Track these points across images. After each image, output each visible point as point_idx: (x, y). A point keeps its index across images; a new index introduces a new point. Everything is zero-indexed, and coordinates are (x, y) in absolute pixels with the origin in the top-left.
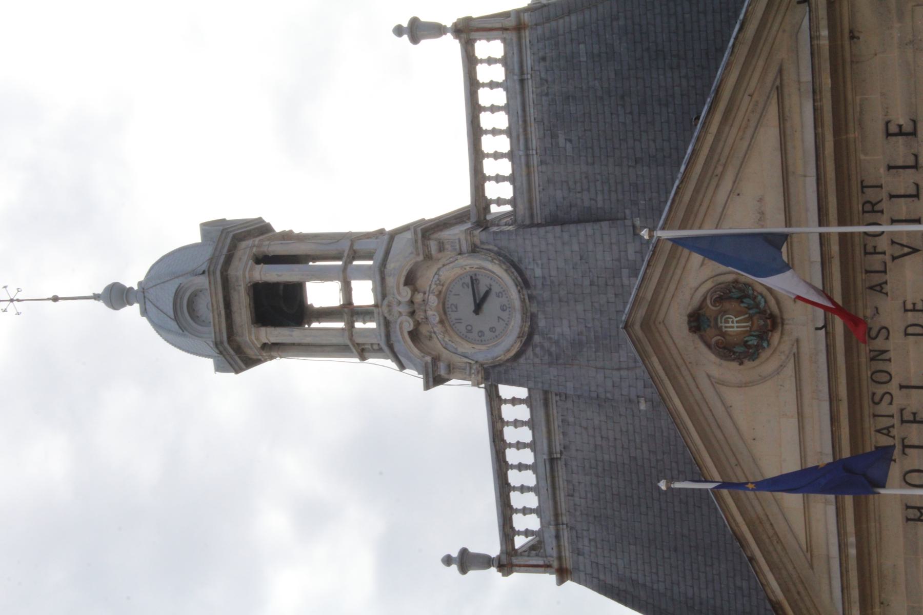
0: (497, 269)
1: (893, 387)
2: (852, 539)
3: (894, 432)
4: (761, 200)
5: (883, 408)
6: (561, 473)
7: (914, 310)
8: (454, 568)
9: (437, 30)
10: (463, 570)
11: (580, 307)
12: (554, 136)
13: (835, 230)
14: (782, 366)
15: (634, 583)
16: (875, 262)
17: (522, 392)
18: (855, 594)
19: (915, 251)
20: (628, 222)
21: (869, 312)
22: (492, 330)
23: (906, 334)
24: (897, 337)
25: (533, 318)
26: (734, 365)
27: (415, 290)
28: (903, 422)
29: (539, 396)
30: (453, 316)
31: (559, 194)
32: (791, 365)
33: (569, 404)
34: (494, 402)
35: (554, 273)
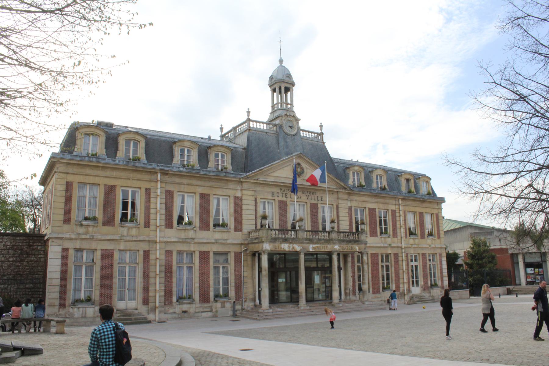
5: (287, 191)
6: (265, 134)
9: (321, 130)
13: (327, 189)
16: (306, 193)
18: (265, 182)
30: (288, 122)
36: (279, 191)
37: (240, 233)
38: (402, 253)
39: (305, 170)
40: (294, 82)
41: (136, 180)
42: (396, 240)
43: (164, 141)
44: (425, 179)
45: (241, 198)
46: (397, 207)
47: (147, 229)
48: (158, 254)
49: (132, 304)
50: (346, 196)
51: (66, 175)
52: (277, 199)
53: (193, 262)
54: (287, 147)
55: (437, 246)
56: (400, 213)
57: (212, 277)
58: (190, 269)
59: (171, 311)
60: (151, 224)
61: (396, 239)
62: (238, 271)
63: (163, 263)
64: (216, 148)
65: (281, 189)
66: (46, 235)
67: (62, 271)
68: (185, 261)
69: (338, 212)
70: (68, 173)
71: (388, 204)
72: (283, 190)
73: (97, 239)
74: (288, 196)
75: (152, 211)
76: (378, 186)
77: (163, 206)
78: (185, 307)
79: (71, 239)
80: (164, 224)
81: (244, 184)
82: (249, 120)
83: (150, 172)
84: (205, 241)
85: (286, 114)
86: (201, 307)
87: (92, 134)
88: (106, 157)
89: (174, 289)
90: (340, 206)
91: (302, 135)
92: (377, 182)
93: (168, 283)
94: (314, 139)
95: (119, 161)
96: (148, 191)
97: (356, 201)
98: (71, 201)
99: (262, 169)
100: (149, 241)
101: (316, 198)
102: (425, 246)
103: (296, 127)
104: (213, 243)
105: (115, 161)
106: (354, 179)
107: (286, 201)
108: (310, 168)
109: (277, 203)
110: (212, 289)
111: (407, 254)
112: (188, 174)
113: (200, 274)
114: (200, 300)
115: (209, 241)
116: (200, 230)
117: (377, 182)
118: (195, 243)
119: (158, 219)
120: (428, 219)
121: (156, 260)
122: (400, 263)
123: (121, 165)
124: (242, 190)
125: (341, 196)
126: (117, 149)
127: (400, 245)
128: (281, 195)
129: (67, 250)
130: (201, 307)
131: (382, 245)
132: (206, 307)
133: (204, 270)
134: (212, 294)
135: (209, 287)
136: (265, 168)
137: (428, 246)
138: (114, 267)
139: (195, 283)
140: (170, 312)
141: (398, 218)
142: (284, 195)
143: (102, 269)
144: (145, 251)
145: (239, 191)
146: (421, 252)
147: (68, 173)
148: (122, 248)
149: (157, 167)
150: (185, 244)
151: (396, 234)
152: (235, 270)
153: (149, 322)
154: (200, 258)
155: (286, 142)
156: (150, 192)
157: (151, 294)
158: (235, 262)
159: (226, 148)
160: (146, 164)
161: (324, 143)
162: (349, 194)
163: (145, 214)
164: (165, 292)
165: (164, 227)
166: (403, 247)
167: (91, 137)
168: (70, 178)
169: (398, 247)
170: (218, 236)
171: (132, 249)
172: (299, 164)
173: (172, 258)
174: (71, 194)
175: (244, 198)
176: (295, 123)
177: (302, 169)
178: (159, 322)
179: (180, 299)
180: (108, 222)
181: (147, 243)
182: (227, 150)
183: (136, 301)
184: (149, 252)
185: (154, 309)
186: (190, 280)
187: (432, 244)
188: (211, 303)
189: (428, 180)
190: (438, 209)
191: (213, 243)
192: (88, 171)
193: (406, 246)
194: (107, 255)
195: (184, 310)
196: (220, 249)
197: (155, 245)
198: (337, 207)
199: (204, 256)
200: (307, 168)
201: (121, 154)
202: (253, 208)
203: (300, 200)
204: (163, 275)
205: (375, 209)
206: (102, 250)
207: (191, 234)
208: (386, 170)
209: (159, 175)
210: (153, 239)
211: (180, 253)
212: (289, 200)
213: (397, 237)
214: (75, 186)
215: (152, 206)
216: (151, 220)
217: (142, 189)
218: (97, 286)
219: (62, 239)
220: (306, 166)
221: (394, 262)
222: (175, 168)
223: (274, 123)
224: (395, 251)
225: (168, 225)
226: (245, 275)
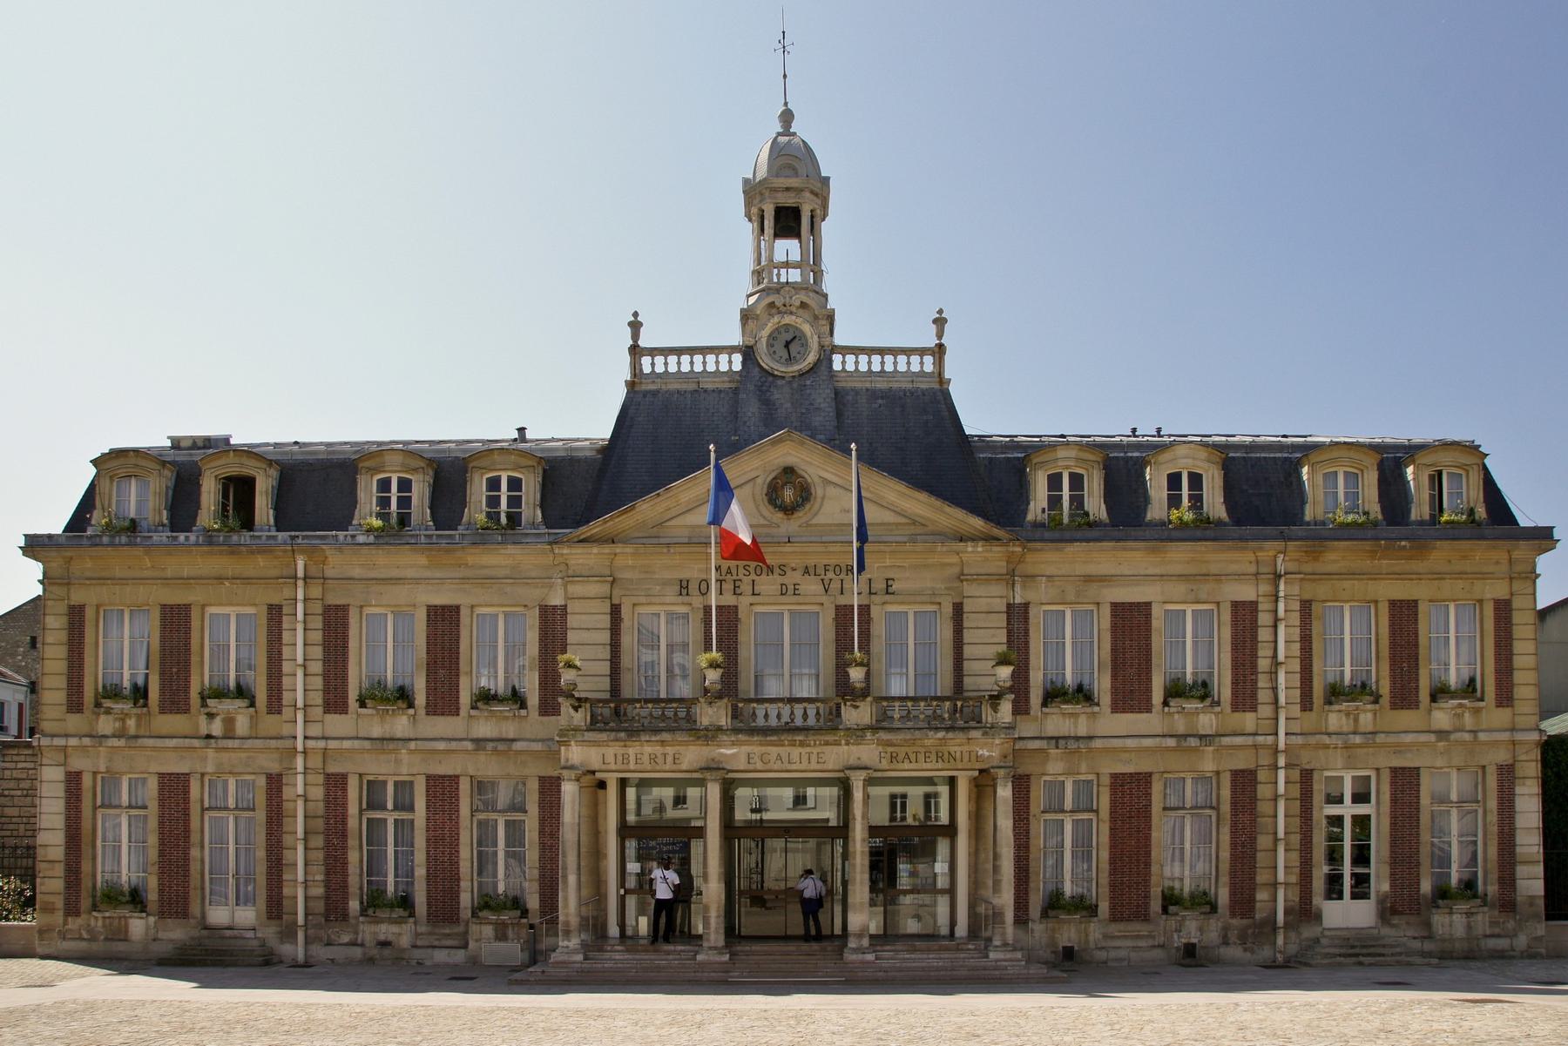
1: (753, 576)
3: (729, 576)
5: (741, 571)
7: (795, 589)
8: (633, 319)
10: (630, 324)
11: (789, 405)
14: (764, 517)
15: (631, 426)
17: (737, 366)
19: (826, 591)
20: (837, 437)
22: (774, 352)
23: (782, 585)
24: (780, 580)
26: (765, 491)
31: (850, 398)
32: (766, 522)
33: (731, 395)
34: (731, 350)
35: (808, 391)
38: (1276, 768)
39: (818, 491)
42: (1248, 720)
46: (1265, 588)
48: (302, 789)
59: (346, 938)
60: (284, 702)
68: (390, 805)
74: (746, 587)
75: (286, 667)
77: (317, 652)
78: (385, 931)
80: (319, 701)
86: (430, 934)
90: (966, 609)
93: (335, 864)
107: (736, 607)
113: (428, 840)
114: (429, 915)
116: (428, 714)
119: (300, 686)
122: (1264, 807)
129: (79, 774)
130: (430, 934)
132: (449, 935)
133: (443, 829)
134: (465, 899)
135: (458, 880)
140: (341, 942)
141: (1264, 635)
142: (728, 586)
143: (161, 823)
144: (270, 777)
151: (1254, 695)
154: (427, 796)
156: (280, 615)
157: (286, 891)
164: (327, 887)
165: (320, 710)
173: (345, 796)
180: (173, 703)
185: (289, 933)
188: (462, 924)
194: (174, 788)
195: (382, 937)
198: (958, 610)
202: (605, 637)
204: (318, 841)
205: (1148, 604)
206: (161, 776)
207: (400, 724)
212: (744, 602)
213: (1254, 709)
218: (153, 865)
221: (1234, 804)
224: (1242, 762)
225: (335, 702)
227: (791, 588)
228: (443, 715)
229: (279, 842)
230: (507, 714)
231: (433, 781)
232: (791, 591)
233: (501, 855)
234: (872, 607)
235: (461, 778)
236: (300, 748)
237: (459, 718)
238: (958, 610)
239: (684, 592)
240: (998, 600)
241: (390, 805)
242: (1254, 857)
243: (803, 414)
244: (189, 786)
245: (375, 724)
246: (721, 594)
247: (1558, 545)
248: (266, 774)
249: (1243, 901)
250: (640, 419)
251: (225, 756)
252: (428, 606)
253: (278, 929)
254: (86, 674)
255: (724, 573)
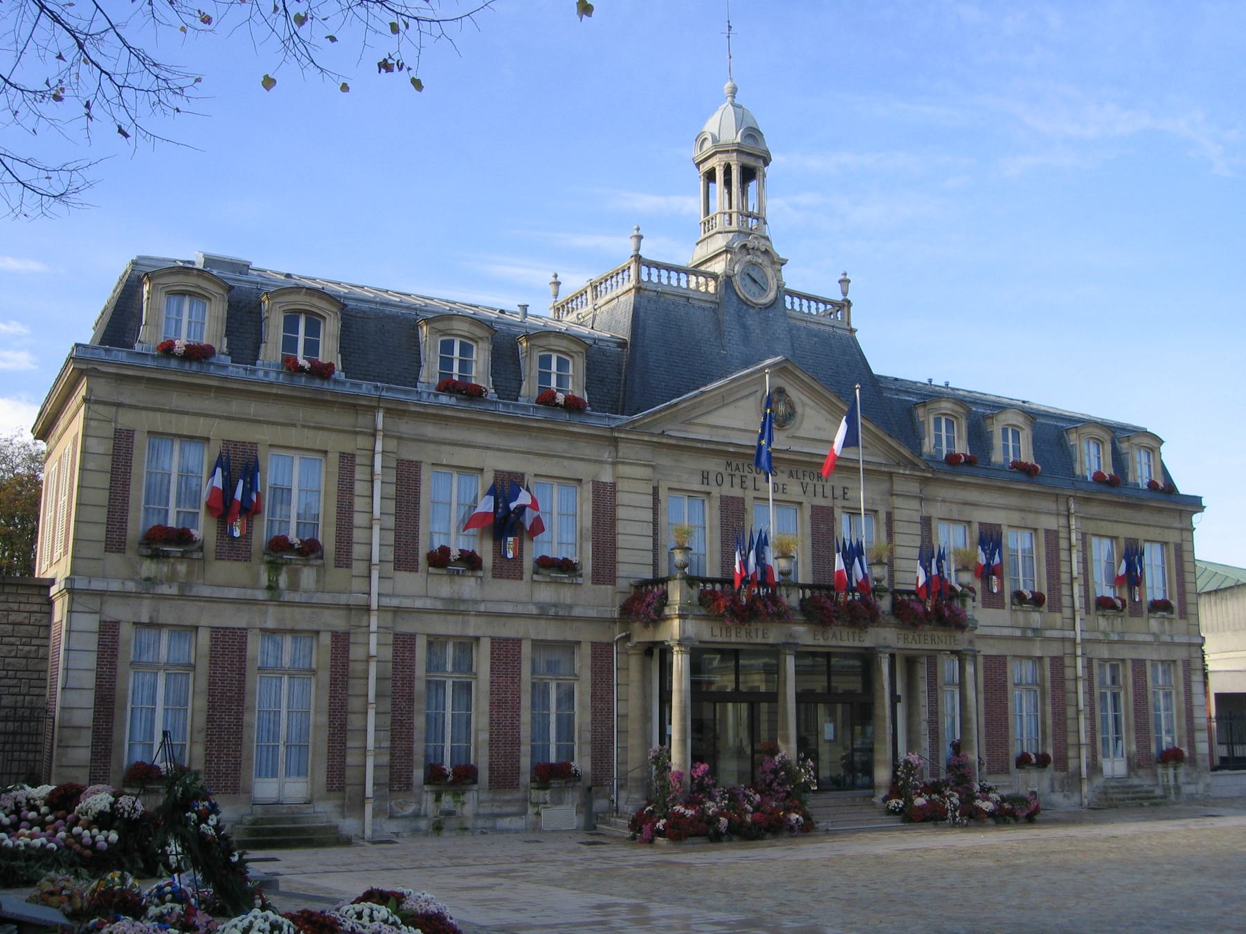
0: (772, 295)
1: (754, 474)
2: (704, 446)
4: (824, 430)
5: (746, 469)
6: (682, 301)
9: (845, 294)
11: (758, 331)
12: (816, 336)
16: (800, 475)
18: (682, 443)
19: (805, 493)
21: (782, 468)
22: (745, 285)
25: (754, 308)
27: (763, 252)
28: (742, 476)
29: (713, 299)
36: (722, 470)
37: (609, 587)
38: (1076, 657)
39: (799, 410)
40: (767, 152)
41: (315, 428)
42: (1057, 618)
43: (394, 318)
44: (1145, 441)
45: (614, 485)
46: (1063, 521)
47: (343, 571)
49: (294, 789)
50: (914, 488)
51: (114, 409)
52: (716, 491)
53: (474, 670)
54: (746, 339)
55: (1176, 639)
56: (1070, 539)
57: (526, 716)
58: (464, 689)
59: (410, 810)
60: (355, 556)
61: (1058, 616)
62: (602, 699)
63: (389, 673)
64: (543, 342)
65: (729, 464)
66: (52, 582)
67: (99, 687)
68: (449, 667)
69: (890, 534)
70: (119, 405)
71: (1037, 512)
72: (734, 465)
73: (198, 598)
74: (749, 483)
75: (359, 519)
76: (1006, 460)
79: (124, 595)
81: (621, 446)
82: (638, 259)
83: (354, 406)
84: (509, 609)
85: (744, 246)
86: (493, 800)
87: (190, 294)
88: (227, 360)
89: (419, 747)
91: (788, 306)
92: (1006, 447)
93: (399, 729)
94: (823, 320)
95: (267, 373)
96: (347, 461)
97: (944, 501)
98: (126, 484)
99: (676, 404)
100: (348, 607)
101: (828, 492)
102: (1141, 638)
103: (773, 284)
104: (530, 616)
105: (254, 372)
106: (938, 438)
107: (743, 499)
108: (812, 404)
109: (717, 503)
110: (525, 749)
111: (1090, 661)
112: (462, 415)
113: (491, 704)
115: (520, 609)
116: (494, 576)
117: (1006, 447)
118: (479, 614)
120: (1153, 558)
121: (367, 661)
122: (1069, 685)
123: (271, 383)
124: (614, 464)
125: (899, 486)
126: (258, 340)
127: (1070, 634)
128: (727, 479)
129: (115, 625)
131: (1018, 633)
132: (509, 801)
134: (525, 762)
135: (519, 744)
136: (685, 400)
137: (1149, 638)
138: (248, 678)
139: (477, 730)
141: (1064, 555)
142: (737, 480)
143: (212, 683)
144: (336, 636)
145: (609, 468)
146: (1128, 654)
147: (119, 405)
148: (270, 624)
149: (373, 392)
150: (450, 618)
152: (594, 696)
153: (346, 842)
155: (744, 326)
156: (353, 465)
157: (352, 759)
158: (594, 672)
159: (572, 341)
160: (343, 383)
161: (852, 331)
162: (925, 481)
163: (339, 528)
164: (392, 755)
166: (1079, 640)
167: (187, 300)
168: (126, 419)
169: (1063, 640)
170: (546, 594)
171: (299, 627)
172: (781, 391)
173: (413, 658)
174: (128, 464)
175: (621, 485)
176: (769, 272)
177: (791, 406)
178: (374, 843)
179: (435, 775)
181: (343, 613)
182: (574, 347)
183: (309, 779)
184: (348, 640)
186: (463, 724)
187: (1164, 633)
189: (1154, 444)
190: (1182, 529)
191: (530, 616)
192: (176, 400)
193: (1087, 636)
196: (550, 632)
197: (365, 617)
198: (889, 516)
199: (506, 652)
200: (804, 405)
201: (272, 351)
202: (648, 516)
203: (783, 497)
204: (387, 705)
206: (214, 630)
207: (468, 587)
208: (1032, 415)
209: (380, 417)
210: (360, 599)
211: (435, 642)
212: (750, 495)
213: (1060, 611)
214: (141, 441)
215: (359, 504)
216: (355, 545)
217: (330, 455)
219: (101, 594)
220: (803, 398)
221: (1052, 682)
222: (425, 396)
223: (710, 270)
225: (404, 558)
226: (622, 712)
227: (781, 487)
228: (508, 578)
229: (344, 706)
230: (566, 581)
231: (497, 643)
232: (781, 490)
233: (553, 718)
234: (835, 509)
235: (524, 642)
236: (374, 606)
237: (523, 582)
238: (889, 516)
239: (705, 481)
240: (915, 513)
241: (449, 667)
242: (1065, 724)
243: (768, 340)
244: (246, 643)
245: (444, 587)
246: (732, 486)
247: (1205, 510)
248: (332, 632)
249: (1062, 762)
250: (650, 322)
251: (287, 611)
252: (495, 471)
253: (338, 802)
254: (130, 509)
255: (734, 468)
